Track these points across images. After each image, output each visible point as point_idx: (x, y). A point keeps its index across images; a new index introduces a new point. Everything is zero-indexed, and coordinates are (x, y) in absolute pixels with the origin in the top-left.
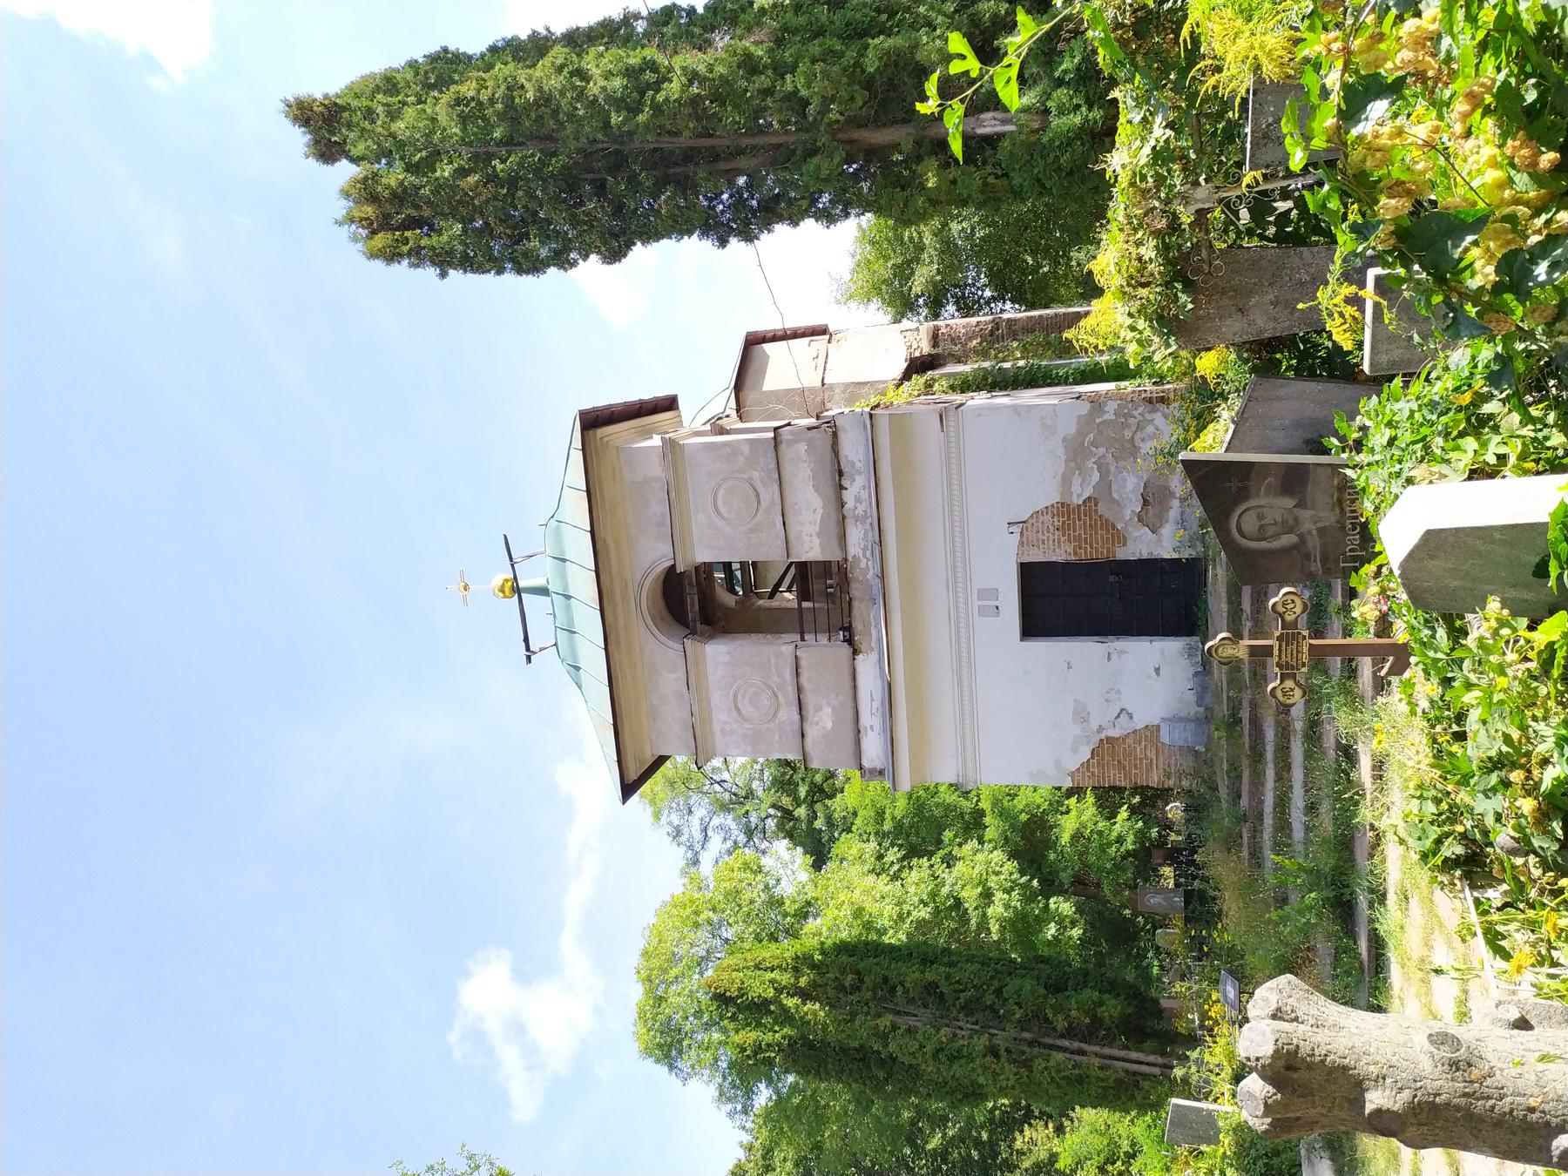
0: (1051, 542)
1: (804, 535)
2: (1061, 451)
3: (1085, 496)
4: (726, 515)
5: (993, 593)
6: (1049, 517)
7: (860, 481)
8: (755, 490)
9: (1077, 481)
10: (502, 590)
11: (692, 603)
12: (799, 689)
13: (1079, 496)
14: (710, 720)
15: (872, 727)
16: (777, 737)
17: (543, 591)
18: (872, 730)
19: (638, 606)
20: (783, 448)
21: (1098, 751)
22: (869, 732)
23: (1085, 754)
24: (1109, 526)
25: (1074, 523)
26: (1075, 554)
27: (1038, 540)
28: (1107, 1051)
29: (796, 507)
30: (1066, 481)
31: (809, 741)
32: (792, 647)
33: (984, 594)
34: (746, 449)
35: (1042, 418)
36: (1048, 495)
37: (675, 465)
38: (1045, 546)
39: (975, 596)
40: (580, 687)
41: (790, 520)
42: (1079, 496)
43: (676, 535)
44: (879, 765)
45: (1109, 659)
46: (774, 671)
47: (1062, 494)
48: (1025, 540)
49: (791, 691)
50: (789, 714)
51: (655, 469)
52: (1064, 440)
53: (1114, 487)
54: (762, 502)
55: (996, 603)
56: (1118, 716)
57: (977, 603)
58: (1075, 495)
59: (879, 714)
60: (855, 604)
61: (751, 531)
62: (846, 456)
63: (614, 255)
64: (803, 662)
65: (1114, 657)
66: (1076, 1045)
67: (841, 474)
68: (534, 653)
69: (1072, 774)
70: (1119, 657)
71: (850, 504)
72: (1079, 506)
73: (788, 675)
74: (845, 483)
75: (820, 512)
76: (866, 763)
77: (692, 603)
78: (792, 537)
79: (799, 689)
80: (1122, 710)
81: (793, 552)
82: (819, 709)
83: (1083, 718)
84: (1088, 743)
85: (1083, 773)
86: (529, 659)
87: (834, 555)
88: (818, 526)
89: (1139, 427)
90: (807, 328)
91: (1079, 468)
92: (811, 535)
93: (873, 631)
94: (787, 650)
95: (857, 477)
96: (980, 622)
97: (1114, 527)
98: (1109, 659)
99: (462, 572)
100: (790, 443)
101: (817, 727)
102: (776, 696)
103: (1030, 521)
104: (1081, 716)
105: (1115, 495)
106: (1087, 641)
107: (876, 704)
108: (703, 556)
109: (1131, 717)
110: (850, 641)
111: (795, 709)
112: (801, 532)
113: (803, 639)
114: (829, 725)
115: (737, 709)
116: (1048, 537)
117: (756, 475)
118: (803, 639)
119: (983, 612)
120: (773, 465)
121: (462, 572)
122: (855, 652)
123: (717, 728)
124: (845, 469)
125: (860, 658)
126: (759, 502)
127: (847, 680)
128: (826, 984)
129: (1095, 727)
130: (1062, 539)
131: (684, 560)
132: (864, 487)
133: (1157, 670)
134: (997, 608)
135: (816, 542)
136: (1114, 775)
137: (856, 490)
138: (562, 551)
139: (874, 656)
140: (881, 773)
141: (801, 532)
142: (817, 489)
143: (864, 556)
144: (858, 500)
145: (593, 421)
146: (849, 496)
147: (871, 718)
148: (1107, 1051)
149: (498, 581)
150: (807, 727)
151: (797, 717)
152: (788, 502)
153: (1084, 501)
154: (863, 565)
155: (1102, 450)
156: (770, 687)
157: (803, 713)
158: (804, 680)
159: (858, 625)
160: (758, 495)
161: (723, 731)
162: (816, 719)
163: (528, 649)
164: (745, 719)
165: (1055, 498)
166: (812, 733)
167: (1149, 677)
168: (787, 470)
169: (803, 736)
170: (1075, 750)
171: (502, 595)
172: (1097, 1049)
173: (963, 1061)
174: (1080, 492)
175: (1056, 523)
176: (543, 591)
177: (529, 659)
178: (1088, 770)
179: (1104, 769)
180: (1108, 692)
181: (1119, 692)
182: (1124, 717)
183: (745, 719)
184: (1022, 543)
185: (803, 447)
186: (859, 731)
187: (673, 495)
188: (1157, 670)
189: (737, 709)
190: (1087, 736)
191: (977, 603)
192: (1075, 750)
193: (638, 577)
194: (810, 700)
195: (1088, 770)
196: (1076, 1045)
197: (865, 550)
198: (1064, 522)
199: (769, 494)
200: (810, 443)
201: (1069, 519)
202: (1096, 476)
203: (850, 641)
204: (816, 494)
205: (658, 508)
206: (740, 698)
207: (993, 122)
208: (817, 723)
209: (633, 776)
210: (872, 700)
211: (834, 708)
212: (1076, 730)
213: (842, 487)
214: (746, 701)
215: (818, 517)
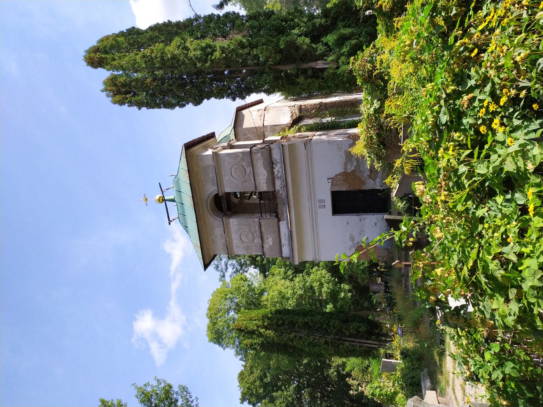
1: (261, 183)
2: (344, 156)
3: (352, 169)
4: (235, 177)
5: (323, 201)
6: (341, 176)
7: (279, 165)
8: (244, 168)
9: (349, 165)
10: (159, 200)
11: (224, 205)
12: (261, 232)
13: (350, 170)
14: (232, 243)
16: (254, 248)
17: (173, 200)
19: (207, 207)
20: (253, 155)
22: (284, 245)
24: (360, 179)
26: (349, 188)
28: (362, 341)
30: (346, 165)
31: (265, 249)
32: (258, 219)
33: (320, 201)
34: (241, 155)
35: (337, 145)
36: (339, 170)
37: (217, 161)
39: (317, 202)
40: (188, 233)
41: (256, 179)
43: (219, 182)
44: (288, 256)
47: (345, 169)
49: (258, 232)
50: (258, 240)
51: (210, 162)
53: (361, 167)
55: (324, 204)
57: (318, 204)
58: (349, 170)
60: (279, 205)
61: (243, 182)
63: (197, 102)
64: (262, 224)
65: (362, 220)
66: (352, 339)
67: (273, 163)
68: (171, 221)
71: (276, 173)
72: (350, 173)
73: (257, 228)
74: (274, 166)
75: (266, 175)
76: (284, 255)
77: (224, 205)
78: (257, 183)
79: (261, 232)
81: (258, 188)
82: (268, 238)
84: (354, 247)
86: (170, 224)
87: (271, 189)
90: (256, 101)
91: (350, 161)
93: (285, 214)
94: (257, 220)
95: (278, 164)
96: (319, 210)
97: (361, 179)
99: (145, 195)
100: (256, 153)
104: (352, 239)
105: (362, 169)
106: (352, 215)
107: (287, 237)
108: (228, 190)
110: (277, 216)
111: (260, 239)
112: (260, 182)
113: (262, 216)
114: (271, 244)
115: (241, 239)
117: (244, 164)
118: (262, 216)
119: (320, 207)
120: (250, 160)
121: (145, 195)
122: (279, 220)
123: (234, 245)
124: (274, 162)
125: (281, 222)
126: (246, 173)
127: (276, 229)
128: (273, 325)
129: (356, 242)
131: (221, 191)
132: (280, 168)
133: (376, 224)
135: (265, 185)
137: (277, 169)
138: (180, 189)
139: (285, 222)
140: (289, 258)
141: (260, 182)
143: (281, 190)
144: (278, 172)
145: (189, 146)
146: (276, 171)
147: (285, 241)
148: (362, 341)
149: (157, 197)
150: (264, 244)
151: (260, 241)
152: (256, 172)
154: (281, 192)
156: (251, 232)
158: (263, 229)
159: (280, 212)
160: (245, 170)
161: (237, 247)
163: (169, 220)
164: (244, 243)
166: (266, 246)
167: (373, 226)
168: (255, 162)
169: (263, 247)
170: (350, 250)
172: (358, 340)
173: (317, 346)
174: (350, 168)
176: (173, 200)
177: (170, 224)
181: (363, 231)
183: (244, 243)
184: (332, 185)
185: (260, 154)
186: (281, 246)
187: (217, 171)
188: (376, 224)
189: (241, 239)
191: (318, 204)
192: (350, 250)
193: (206, 197)
194: (265, 236)
196: (352, 339)
197: (281, 188)
199: (249, 170)
200: (262, 153)
202: (355, 163)
203: (277, 216)
205: (212, 175)
207: (321, 64)
208: (267, 243)
209: (207, 262)
211: (273, 238)
212: (351, 243)
213: (273, 168)
214: (244, 237)
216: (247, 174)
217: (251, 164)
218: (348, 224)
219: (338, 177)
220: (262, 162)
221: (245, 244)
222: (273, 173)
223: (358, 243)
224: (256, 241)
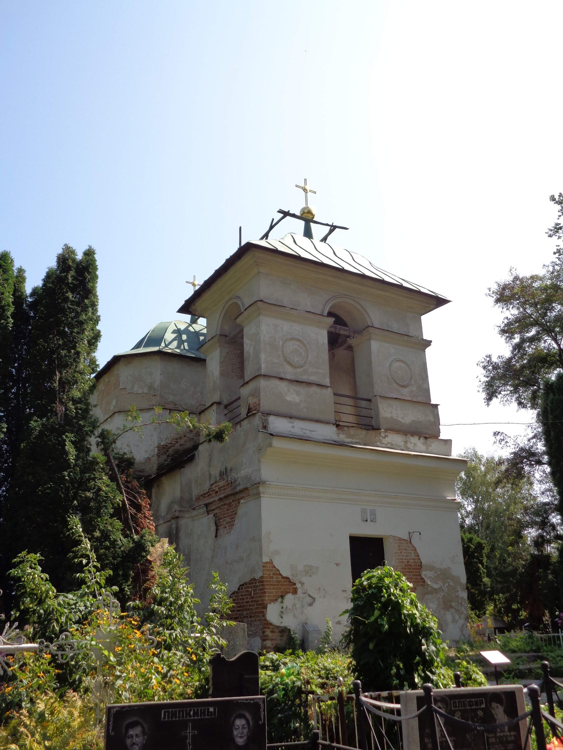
0: (401, 557)
6: (413, 557)
12: (309, 384)
13: (425, 575)
15: (293, 427)
16: (275, 361)
18: (293, 427)
21: (286, 582)
22: (291, 425)
23: (285, 573)
25: (412, 572)
27: (402, 549)
29: (404, 408)
31: (277, 382)
33: (373, 513)
38: (399, 554)
42: (425, 575)
45: (343, 591)
46: (315, 370)
48: (401, 542)
50: (289, 372)
52: (449, 568)
53: (430, 596)
54: (402, 389)
55: (369, 520)
56: (310, 596)
59: (302, 433)
60: (364, 432)
62: (433, 442)
64: (324, 391)
69: (271, 562)
70: (345, 597)
73: (313, 379)
75: (403, 421)
76: (271, 419)
78: (390, 401)
79: (309, 384)
80: (314, 599)
82: (298, 394)
83: (308, 572)
84: (293, 575)
85: (271, 571)
88: (396, 418)
89: (457, 611)
92: (391, 413)
98: (343, 591)
101: (286, 390)
102: (301, 367)
103: (411, 546)
104: (310, 571)
107: (308, 433)
109: (311, 605)
111: (293, 378)
114: (288, 398)
116: (403, 556)
119: (364, 511)
126: (402, 386)
130: (403, 564)
134: (367, 521)
135: (389, 415)
136: (272, 593)
142: (413, 422)
153: (422, 578)
155: (446, 589)
157: (295, 383)
158: (314, 389)
162: (291, 390)
165: (424, 562)
166: (283, 386)
171: (306, 211)
175: (411, 561)
178: (274, 574)
179: (275, 585)
180: (324, 589)
181: (324, 597)
182: (309, 600)
184: (400, 539)
186: (291, 418)
187: (406, 338)
189: (292, 339)
190: (296, 574)
194: (302, 390)
195: (274, 574)
198: (411, 566)
201: (413, 569)
204: (411, 421)
205: (395, 326)
206: (298, 343)
210: (311, 431)
215: (400, 419)
216: (401, 389)
217: (415, 400)
218: (337, 565)
219: (412, 552)
220: (421, 420)
221: (281, 343)
222: (413, 434)
223: (303, 584)
224: (289, 368)
